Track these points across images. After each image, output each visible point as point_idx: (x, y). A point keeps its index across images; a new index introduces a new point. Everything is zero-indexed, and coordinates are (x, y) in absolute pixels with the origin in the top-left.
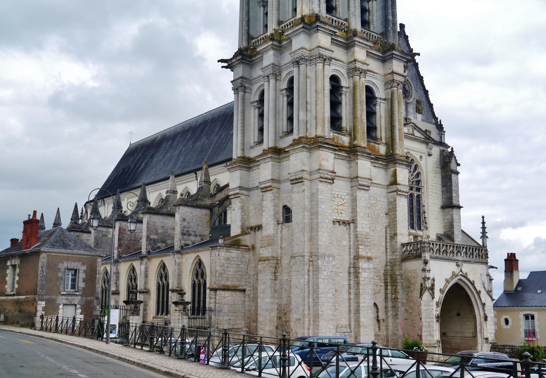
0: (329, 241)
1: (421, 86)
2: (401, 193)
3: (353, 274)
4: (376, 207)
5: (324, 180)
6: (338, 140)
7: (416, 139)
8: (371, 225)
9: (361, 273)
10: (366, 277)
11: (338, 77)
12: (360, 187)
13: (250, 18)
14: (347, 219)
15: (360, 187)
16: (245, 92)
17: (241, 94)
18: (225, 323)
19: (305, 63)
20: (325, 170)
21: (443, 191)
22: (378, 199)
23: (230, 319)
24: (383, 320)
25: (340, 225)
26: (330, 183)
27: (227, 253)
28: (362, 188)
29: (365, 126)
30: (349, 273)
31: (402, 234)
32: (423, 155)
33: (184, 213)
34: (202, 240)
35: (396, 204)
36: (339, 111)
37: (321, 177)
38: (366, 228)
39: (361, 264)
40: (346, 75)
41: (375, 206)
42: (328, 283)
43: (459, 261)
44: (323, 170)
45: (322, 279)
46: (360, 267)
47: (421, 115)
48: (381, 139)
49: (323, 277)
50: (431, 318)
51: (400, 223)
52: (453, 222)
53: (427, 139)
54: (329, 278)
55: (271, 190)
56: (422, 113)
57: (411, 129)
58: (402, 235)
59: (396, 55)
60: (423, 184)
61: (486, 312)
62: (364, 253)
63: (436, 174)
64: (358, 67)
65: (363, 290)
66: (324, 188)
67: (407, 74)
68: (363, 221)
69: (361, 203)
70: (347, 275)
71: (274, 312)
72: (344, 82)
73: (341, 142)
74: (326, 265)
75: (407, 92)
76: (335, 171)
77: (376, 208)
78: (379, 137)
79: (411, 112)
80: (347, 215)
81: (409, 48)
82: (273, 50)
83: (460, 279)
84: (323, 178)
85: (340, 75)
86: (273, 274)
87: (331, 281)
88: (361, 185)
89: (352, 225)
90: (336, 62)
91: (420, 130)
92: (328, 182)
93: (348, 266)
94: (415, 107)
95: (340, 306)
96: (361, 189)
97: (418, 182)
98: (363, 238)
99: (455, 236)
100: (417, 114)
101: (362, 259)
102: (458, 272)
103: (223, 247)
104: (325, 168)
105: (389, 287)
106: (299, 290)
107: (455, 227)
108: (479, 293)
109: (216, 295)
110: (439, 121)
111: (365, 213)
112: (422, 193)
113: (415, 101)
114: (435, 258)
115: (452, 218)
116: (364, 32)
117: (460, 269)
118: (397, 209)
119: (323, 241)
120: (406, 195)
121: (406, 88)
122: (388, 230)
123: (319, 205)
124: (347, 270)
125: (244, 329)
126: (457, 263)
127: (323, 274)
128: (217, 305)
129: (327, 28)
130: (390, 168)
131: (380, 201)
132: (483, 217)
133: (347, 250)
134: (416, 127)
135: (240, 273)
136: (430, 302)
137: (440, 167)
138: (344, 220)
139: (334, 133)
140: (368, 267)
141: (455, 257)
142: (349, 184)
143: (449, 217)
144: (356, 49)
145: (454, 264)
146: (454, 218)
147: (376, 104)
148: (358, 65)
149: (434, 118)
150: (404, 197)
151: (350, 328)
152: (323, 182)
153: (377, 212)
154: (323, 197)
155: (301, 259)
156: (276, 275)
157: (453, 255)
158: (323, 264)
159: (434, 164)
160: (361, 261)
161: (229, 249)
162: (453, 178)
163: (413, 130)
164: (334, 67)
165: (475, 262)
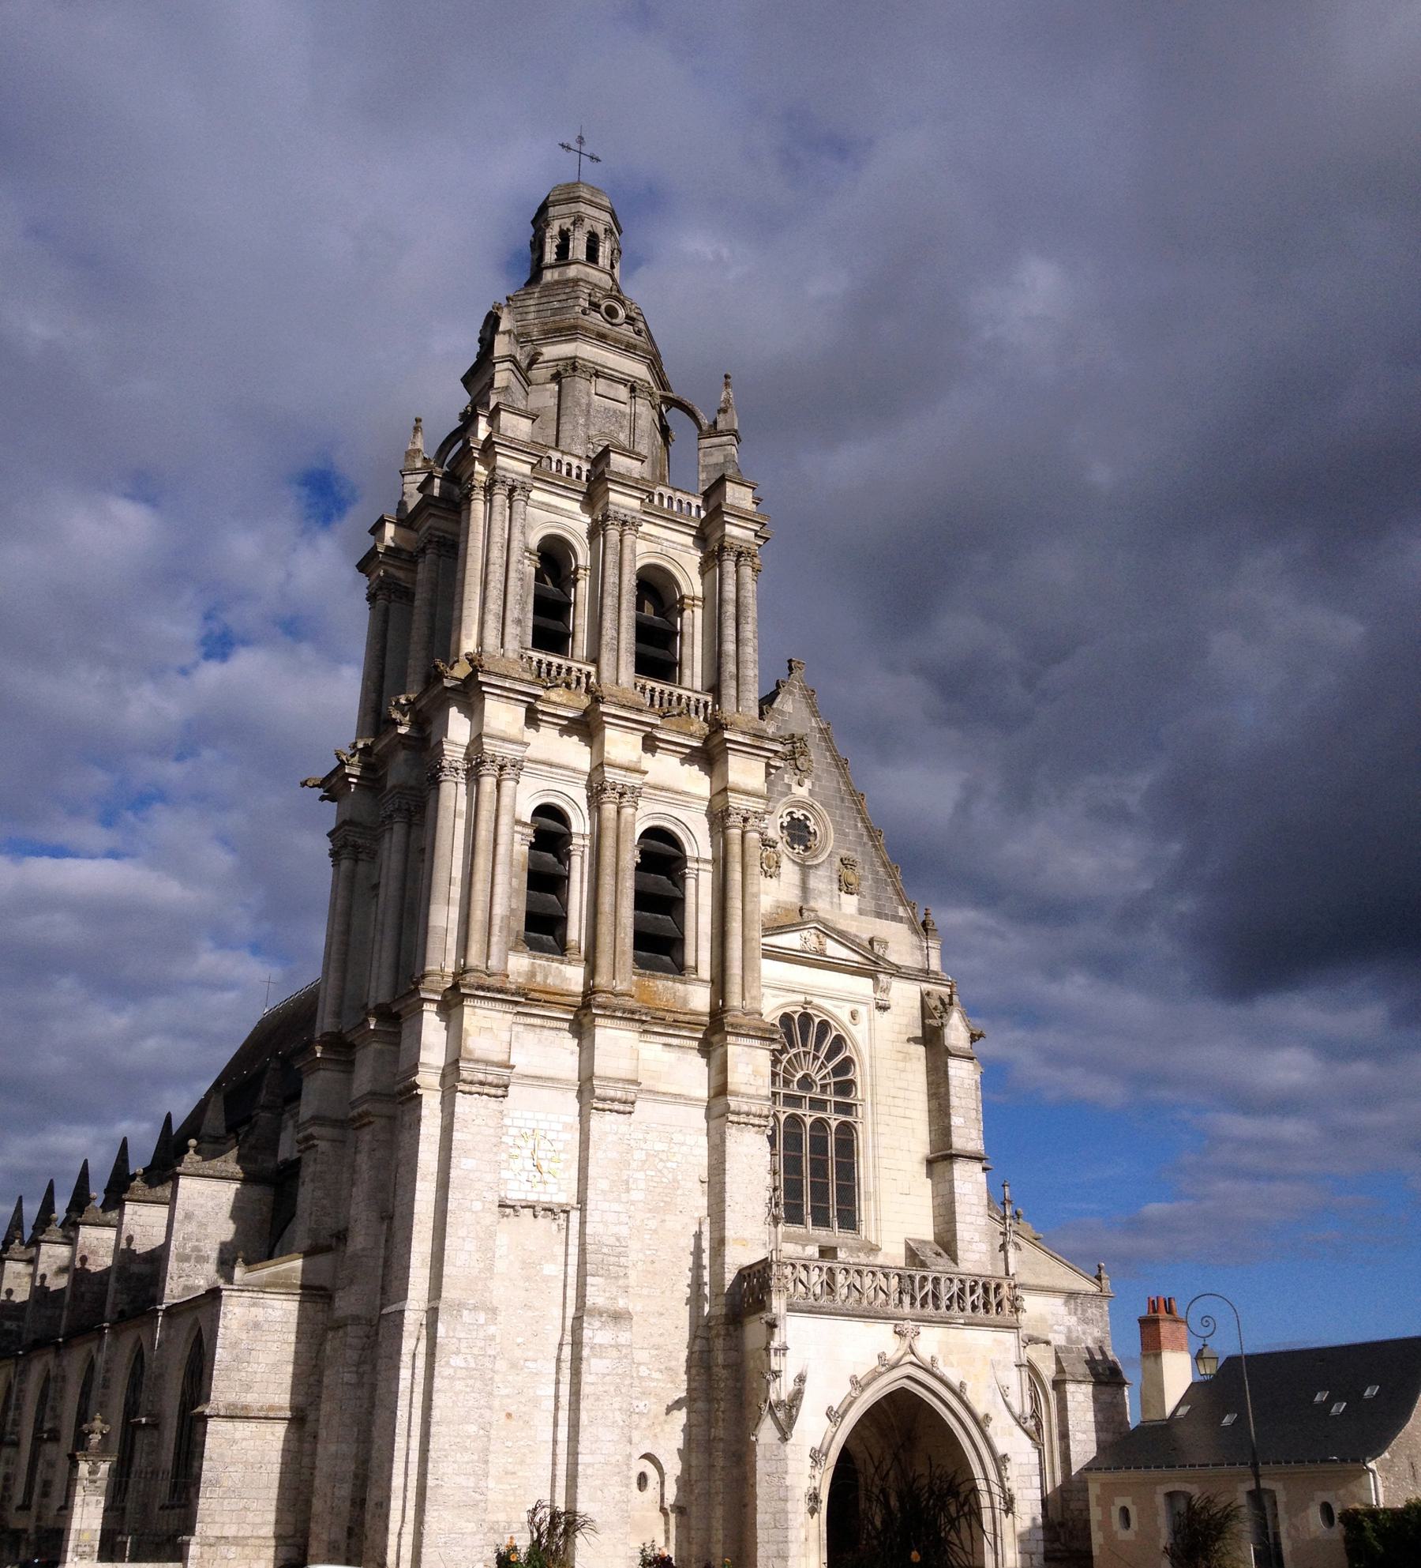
0: (482, 1265)
1: (859, 820)
4: (668, 1160)
5: (474, 1089)
6: (546, 977)
9: (588, 1359)
10: (606, 1371)
12: (600, 1105)
16: (356, 861)
18: (227, 1520)
20: (477, 1061)
22: (678, 1137)
25: (535, 1216)
27: (252, 1309)
29: (626, 935)
31: (744, 1240)
32: (862, 1010)
33: (189, 1198)
35: (724, 1151)
38: (616, 1224)
39: (587, 1334)
40: (584, 804)
41: (665, 1158)
42: (468, 1390)
44: (469, 1060)
47: (855, 898)
48: (696, 968)
50: (780, 1499)
51: (738, 1206)
54: (471, 1378)
55: (370, 1123)
57: (814, 938)
58: (744, 1242)
60: (861, 1093)
61: (1007, 1484)
63: (904, 1060)
64: (611, 781)
65: (592, 1414)
66: (474, 1110)
68: (607, 1204)
69: (605, 1151)
71: (345, 1485)
72: (580, 824)
73: (558, 982)
74: (462, 1335)
75: (812, 838)
76: (512, 1063)
77: (669, 1165)
78: (690, 960)
82: (404, 748)
83: (909, 1377)
84: (471, 1083)
86: (354, 1369)
87: (478, 1384)
88: (604, 1100)
90: (553, 770)
91: (843, 938)
94: (835, 876)
96: (604, 1110)
97: (846, 1088)
99: (960, 1244)
101: (592, 1316)
102: (901, 1353)
104: (478, 1054)
107: (958, 1218)
108: (981, 1423)
111: (614, 1181)
114: (810, 1312)
116: (643, 688)
118: (727, 1166)
119: (458, 1263)
120: (760, 1126)
121: (808, 827)
125: (289, 1541)
126: (896, 1325)
130: (714, 1050)
131: (683, 1144)
136: (779, 1448)
138: (550, 1202)
140: (613, 1343)
141: (891, 1309)
144: (610, 733)
145: (885, 1330)
147: (685, 873)
149: (903, 905)
153: (670, 1176)
154: (469, 1137)
156: (361, 1370)
158: (451, 1334)
159: (900, 1033)
160: (589, 1324)
161: (261, 1295)
162: (951, 1072)
164: (546, 785)
165: (965, 1324)
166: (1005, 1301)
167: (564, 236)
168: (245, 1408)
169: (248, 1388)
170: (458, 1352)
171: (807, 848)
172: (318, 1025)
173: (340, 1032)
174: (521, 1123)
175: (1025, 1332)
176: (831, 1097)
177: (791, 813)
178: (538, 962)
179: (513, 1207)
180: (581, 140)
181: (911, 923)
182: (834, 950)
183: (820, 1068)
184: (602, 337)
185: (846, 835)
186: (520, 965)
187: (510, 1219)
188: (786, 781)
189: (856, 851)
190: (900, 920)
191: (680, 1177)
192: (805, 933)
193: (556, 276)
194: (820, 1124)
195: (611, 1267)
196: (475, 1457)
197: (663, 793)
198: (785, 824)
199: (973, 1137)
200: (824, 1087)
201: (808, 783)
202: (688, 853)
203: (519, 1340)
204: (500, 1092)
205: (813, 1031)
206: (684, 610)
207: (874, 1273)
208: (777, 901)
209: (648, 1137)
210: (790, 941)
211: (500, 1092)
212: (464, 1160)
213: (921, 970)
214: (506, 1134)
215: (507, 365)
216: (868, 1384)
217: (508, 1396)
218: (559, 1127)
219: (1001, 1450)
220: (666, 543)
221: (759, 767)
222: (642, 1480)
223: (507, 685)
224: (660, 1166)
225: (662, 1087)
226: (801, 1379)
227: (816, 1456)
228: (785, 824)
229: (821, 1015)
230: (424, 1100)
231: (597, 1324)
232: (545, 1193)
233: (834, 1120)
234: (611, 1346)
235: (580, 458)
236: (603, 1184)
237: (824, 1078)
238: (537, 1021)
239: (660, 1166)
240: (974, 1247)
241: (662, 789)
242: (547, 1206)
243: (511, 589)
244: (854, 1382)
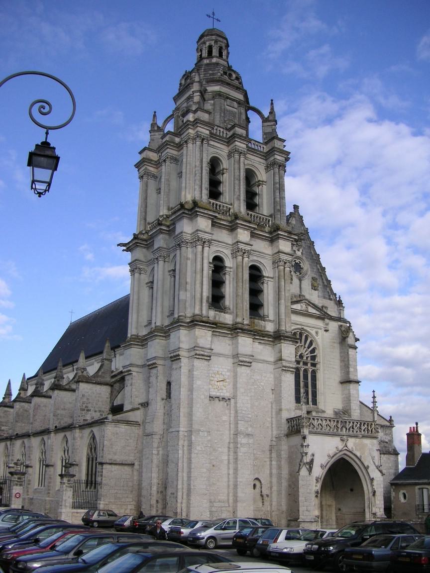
3: (232, 449)
4: (261, 382)
5: (200, 357)
11: (222, 258)
12: (240, 363)
13: (148, 205)
17: (137, 275)
19: (185, 246)
21: (341, 366)
23: (116, 493)
24: (267, 496)
25: (219, 400)
26: (207, 360)
28: (243, 364)
30: (229, 448)
34: (101, 415)
36: (223, 290)
37: (196, 354)
39: (239, 439)
40: (230, 256)
44: (199, 347)
45: (195, 454)
46: (239, 442)
47: (317, 292)
49: (196, 452)
52: (350, 396)
53: (323, 315)
54: (203, 453)
56: (318, 290)
57: (304, 305)
59: (282, 235)
61: (375, 487)
66: (200, 364)
67: (302, 253)
70: (226, 450)
72: (228, 263)
76: (212, 348)
77: (262, 384)
80: (228, 391)
83: (345, 454)
84: (199, 355)
85: (224, 255)
88: (242, 362)
89: (232, 401)
91: (315, 306)
92: (204, 359)
93: (228, 441)
95: (218, 481)
96: (241, 365)
97: (314, 358)
99: (352, 410)
102: (342, 447)
104: (201, 345)
105: (274, 463)
106: (174, 464)
107: (351, 401)
108: (367, 468)
109: (102, 469)
110: (337, 296)
113: (310, 279)
115: (350, 393)
117: (345, 443)
118: (282, 384)
120: (292, 371)
122: (274, 405)
123: (194, 381)
124: (227, 445)
125: (132, 503)
126: (341, 438)
127: (198, 448)
128: (103, 479)
132: (374, 392)
133: (227, 426)
134: (310, 304)
135: (128, 448)
139: (216, 311)
143: (346, 392)
144: (239, 231)
145: (338, 439)
146: (351, 393)
147: (264, 282)
148: (241, 246)
150: (290, 372)
151: (228, 503)
152: (199, 358)
155: (176, 433)
157: (337, 430)
162: (350, 353)
163: (307, 306)
167: (210, 48)
168: (115, 460)
169: (115, 454)
170: (199, 445)
171: (300, 274)
172: (129, 331)
173: (138, 334)
177: (295, 261)
180: (213, 14)
181: (335, 300)
182: (312, 310)
183: (306, 351)
184: (228, 84)
186: (212, 314)
190: (331, 299)
192: (302, 304)
193: (208, 62)
196: (206, 479)
200: (307, 358)
201: (301, 250)
203: (216, 441)
204: (208, 358)
205: (303, 338)
206: (260, 185)
210: (297, 307)
211: (208, 358)
212: (198, 381)
213: (338, 318)
215: (198, 94)
216: (333, 456)
217: (213, 459)
219: (372, 477)
220: (253, 161)
221: (289, 244)
222: (255, 486)
223: (206, 212)
224: (259, 384)
227: (317, 480)
230: (182, 360)
231: (242, 437)
233: (310, 369)
235: (223, 129)
236: (242, 390)
237: (307, 354)
238: (218, 334)
240: (356, 411)
242: (223, 397)
243: (203, 176)
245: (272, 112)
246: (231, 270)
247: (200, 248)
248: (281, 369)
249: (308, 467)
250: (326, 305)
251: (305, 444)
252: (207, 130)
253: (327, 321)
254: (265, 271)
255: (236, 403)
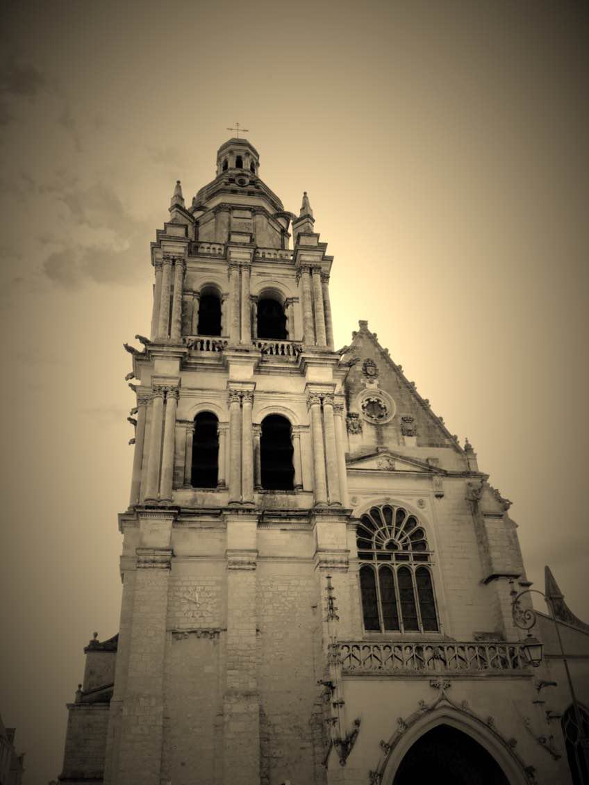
2: (329, 565)
4: (288, 596)
6: (204, 501)
7: (403, 475)
8: (276, 631)
12: (233, 567)
14: (215, 625)
15: (233, 567)
20: (148, 549)
22: (293, 582)
26: (163, 568)
28: (237, 567)
32: (426, 499)
40: (225, 407)
43: (437, 676)
52: (500, 605)
59: (309, 358)
62: (238, 684)
72: (222, 417)
77: (289, 599)
79: (390, 438)
80: (217, 618)
81: (379, 350)
83: (444, 716)
90: (205, 392)
96: (235, 569)
98: (239, 655)
100: (406, 438)
102: (436, 700)
103: (80, 706)
104: (149, 545)
112: (430, 562)
115: (498, 599)
120: (342, 568)
121: (380, 406)
126: (431, 681)
129: (165, 350)
137: (469, 512)
139: (195, 491)
140: (245, 711)
142: (222, 566)
144: (232, 367)
149: (448, 438)
153: (290, 606)
161: (91, 708)
162: (486, 526)
164: (201, 401)
166: (519, 661)
174: (188, 584)
175: (539, 679)
176: (410, 552)
177: (368, 400)
178: (198, 493)
179: (183, 633)
185: (403, 405)
187: (183, 641)
188: (362, 382)
189: (411, 412)
190: (447, 446)
191: (297, 606)
194: (404, 571)
195: (244, 664)
197: (274, 395)
198: (365, 406)
199: (508, 563)
201: (376, 382)
202: (293, 423)
207: (411, 648)
208: (363, 446)
209: (274, 584)
214: (179, 591)
216: (413, 723)
218: (213, 583)
224: (283, 600)
225: (282, 554)
226: (357, 723)
228: (365, 406)
229: (398, 505)
231: (234, 700)
232: (205, 622)
233: (414, 566)
234: (244, 713)
237: (405, 541)
239: (283, 600)
241: (272, 393)
244: (401, 722)
245: (305, 205)
246: (228, 427)
247: (158, 401)
248: (318, 568)
249: (339, 748)
250: (436, 456)
251: (334, 699)
252: (180, 247)
253: (436, 479)
254: (294, 418)
255: (226, 638)
